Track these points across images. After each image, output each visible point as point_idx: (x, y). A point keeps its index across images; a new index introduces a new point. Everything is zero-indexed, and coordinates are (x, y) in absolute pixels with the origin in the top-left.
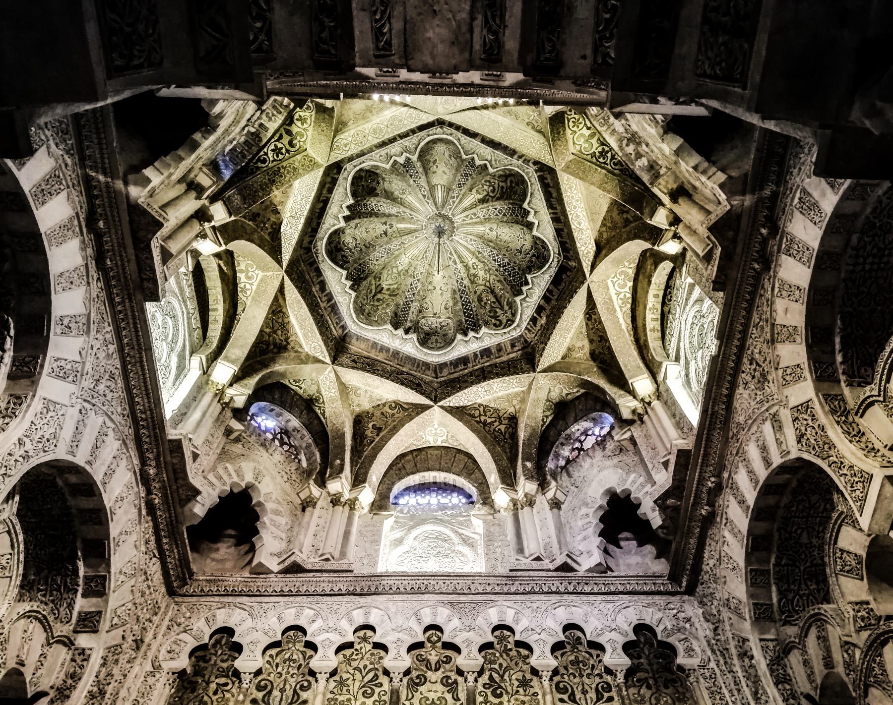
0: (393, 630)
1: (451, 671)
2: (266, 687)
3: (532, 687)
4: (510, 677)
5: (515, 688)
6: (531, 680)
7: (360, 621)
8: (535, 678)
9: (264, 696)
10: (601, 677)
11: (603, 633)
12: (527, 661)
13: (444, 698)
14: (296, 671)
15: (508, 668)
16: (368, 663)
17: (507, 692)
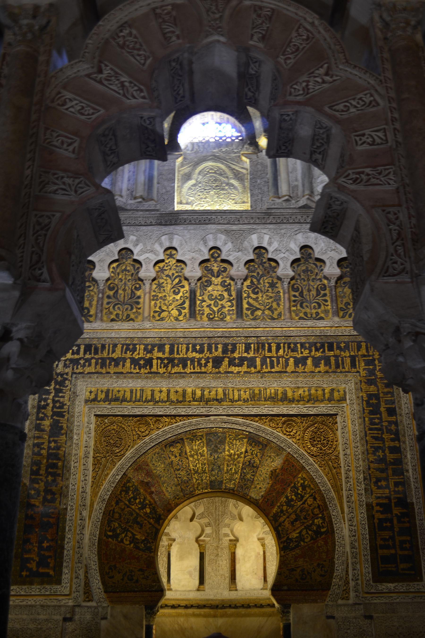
0: (189, 251)
1: (227, 277)
3: (277, 287)
4: (264, 281)
5: (266, 288)
6: (277, 283)
7: (167, 245)
8: (279, 282)
9: (114, 293)
10: (320, 280)
11: (326, 252)
12: (275, 270)
13: (222, 295)
14: (130, 278)
15: (262, 276)
16: (174, 272)
17: (262, 291)
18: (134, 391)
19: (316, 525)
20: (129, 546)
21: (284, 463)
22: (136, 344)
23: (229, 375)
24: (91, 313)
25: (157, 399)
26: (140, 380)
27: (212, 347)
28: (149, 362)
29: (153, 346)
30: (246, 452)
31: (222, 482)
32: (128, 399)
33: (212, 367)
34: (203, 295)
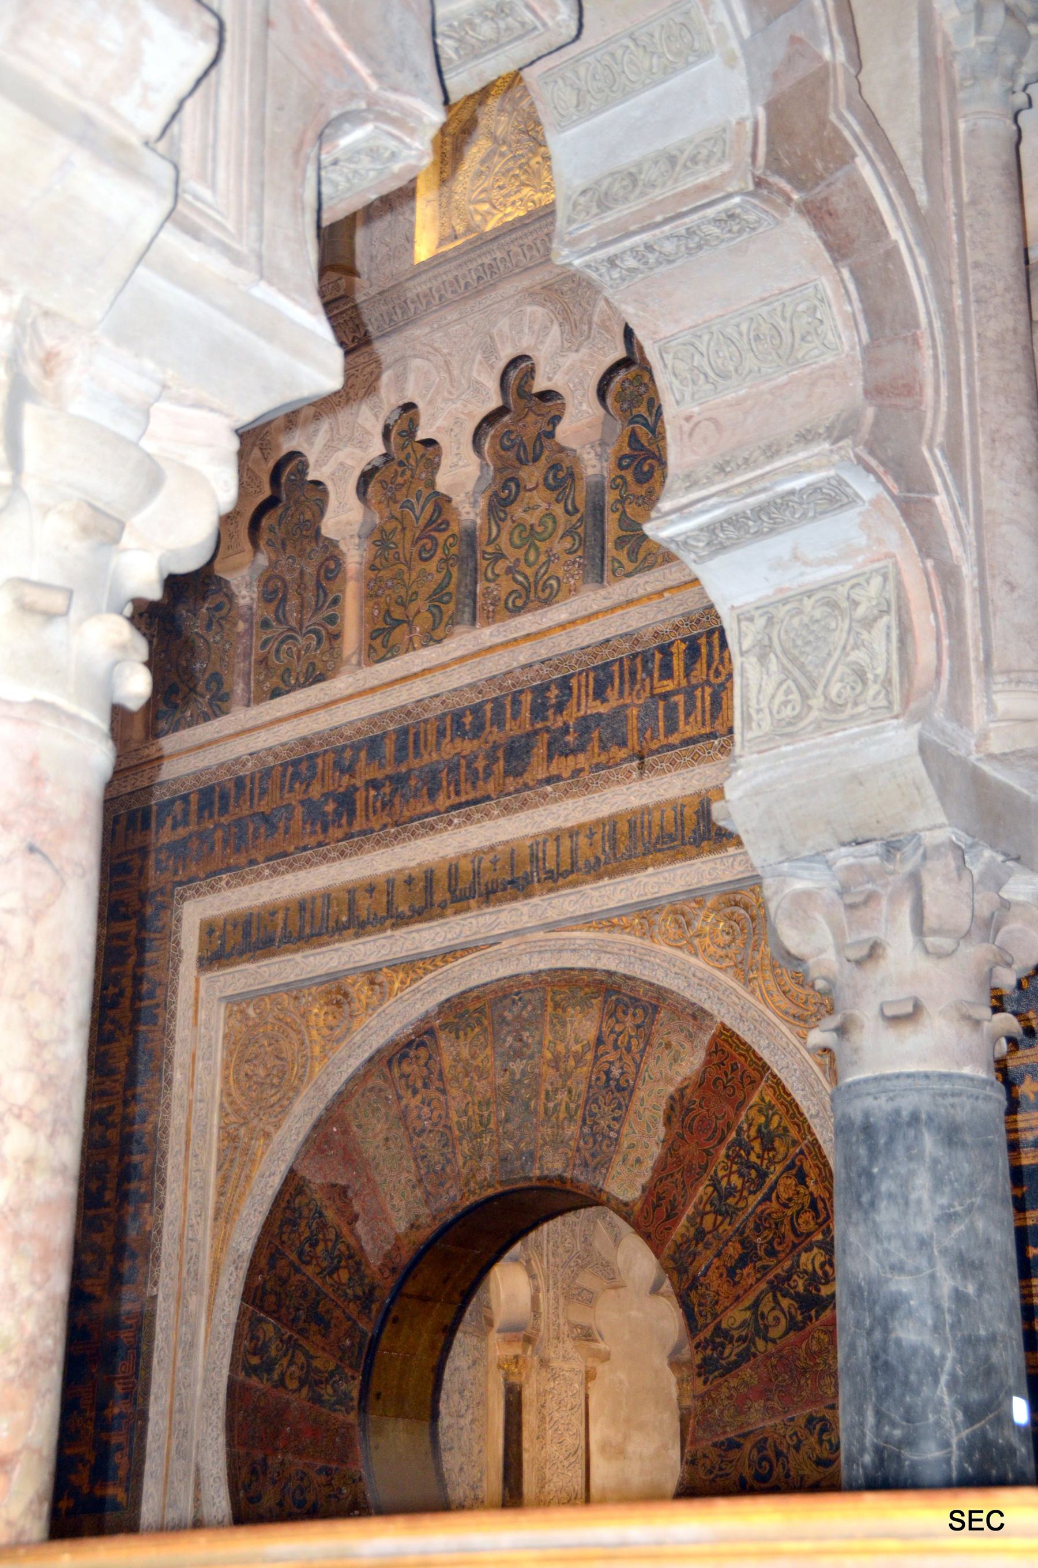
2: (275, 591)
9: (276, 612)
18: (309, 906)
19: (805, 1272)
20: (296, 1395)
21: (708, 1063)
22: (317, 755)
23: (549, 789)
24: (225, 689)
25: (363, 915)
26: (323, 868)
27: (503, 706)
28: (346, 802)
29: (356, 748)
30: (600, 1041)
31: (532, 1155)
32: (295, 935)
33: (507, 773)
34: (498, 535)
